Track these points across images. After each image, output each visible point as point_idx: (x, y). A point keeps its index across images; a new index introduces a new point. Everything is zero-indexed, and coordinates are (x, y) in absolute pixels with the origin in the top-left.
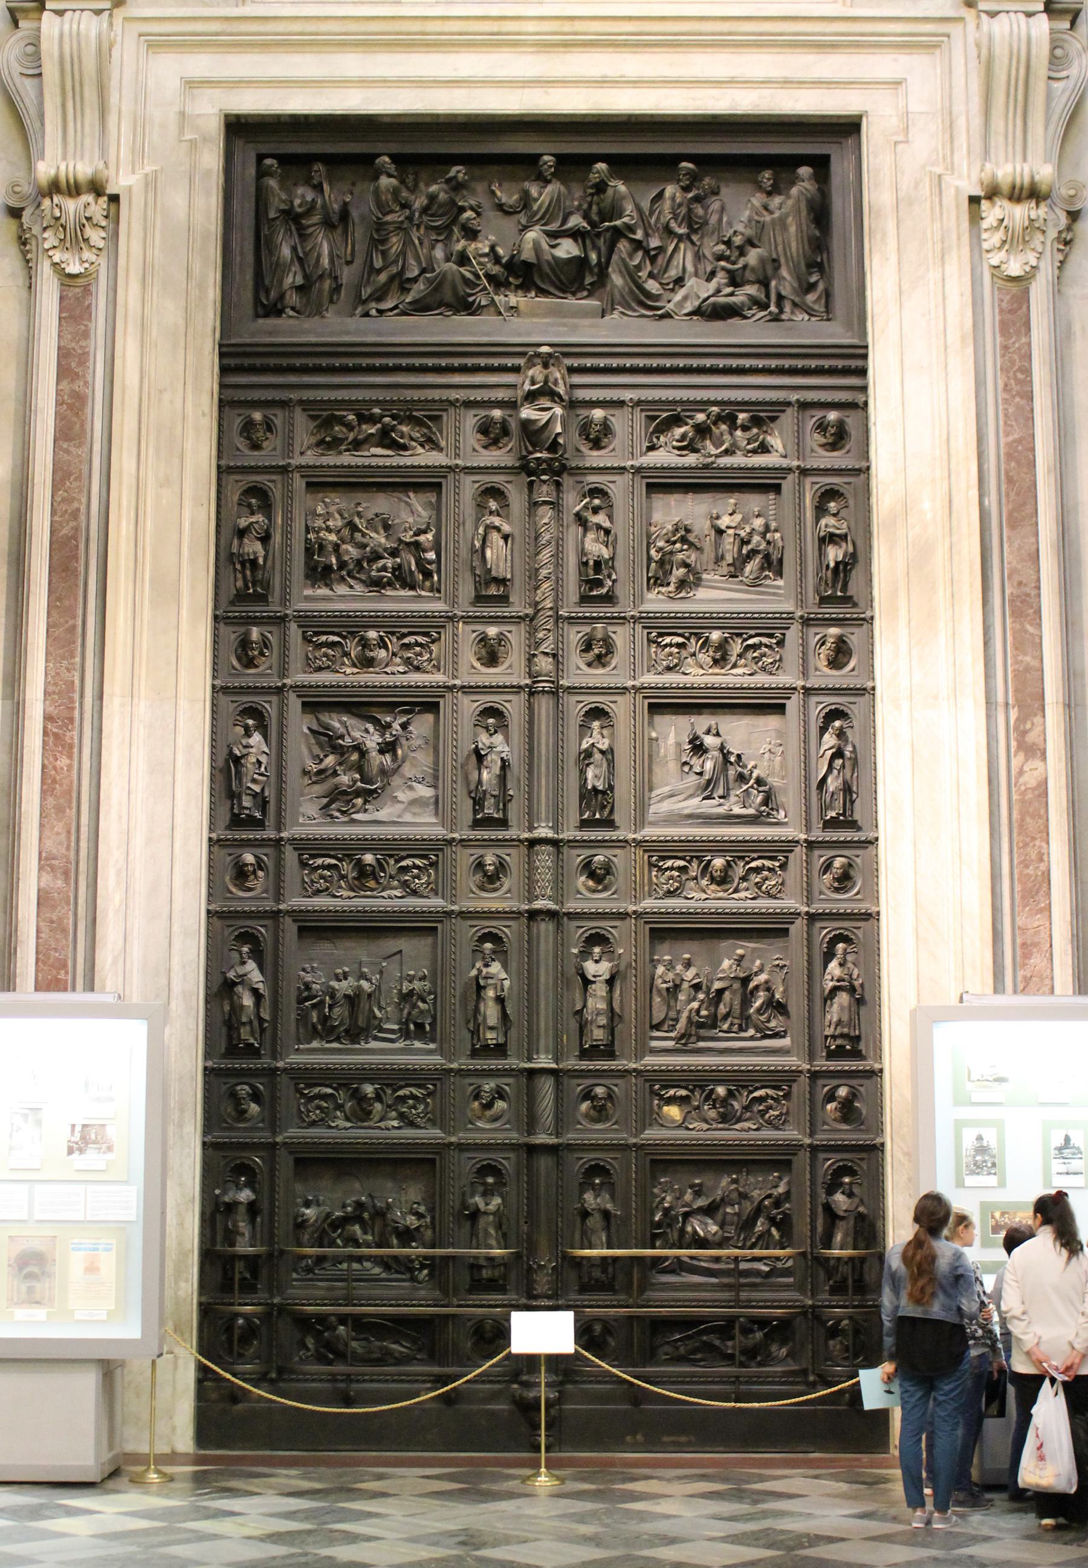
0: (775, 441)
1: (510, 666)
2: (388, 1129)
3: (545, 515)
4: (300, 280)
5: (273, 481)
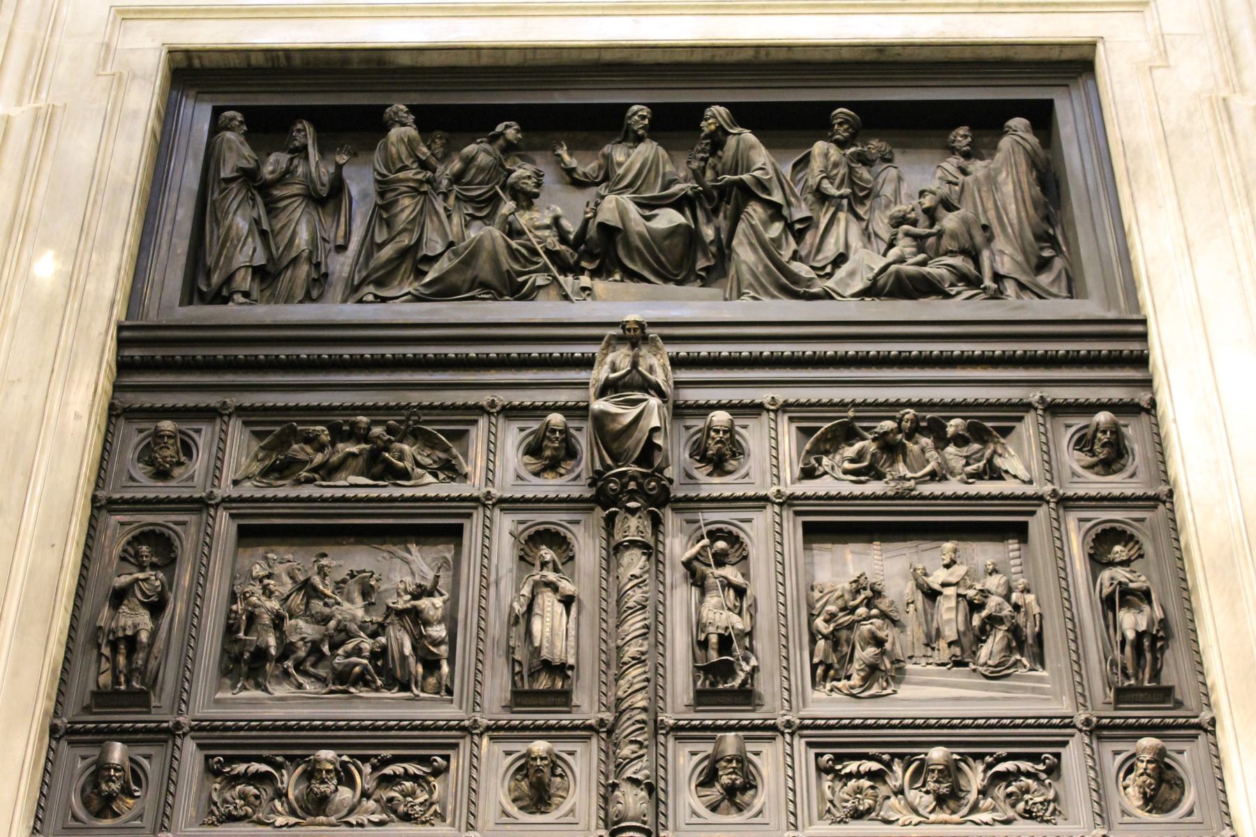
0: (1010, 462)
1: (572, 811)
4: (260, 259)
5: (184, 523)
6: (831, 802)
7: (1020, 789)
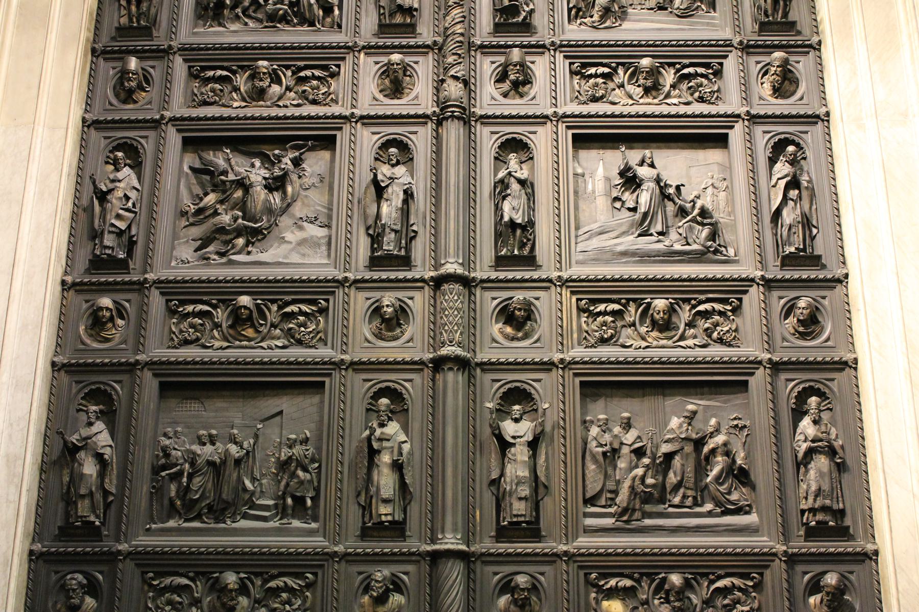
1: (417, 97)
6: (579, 92)
7: (697, 84)
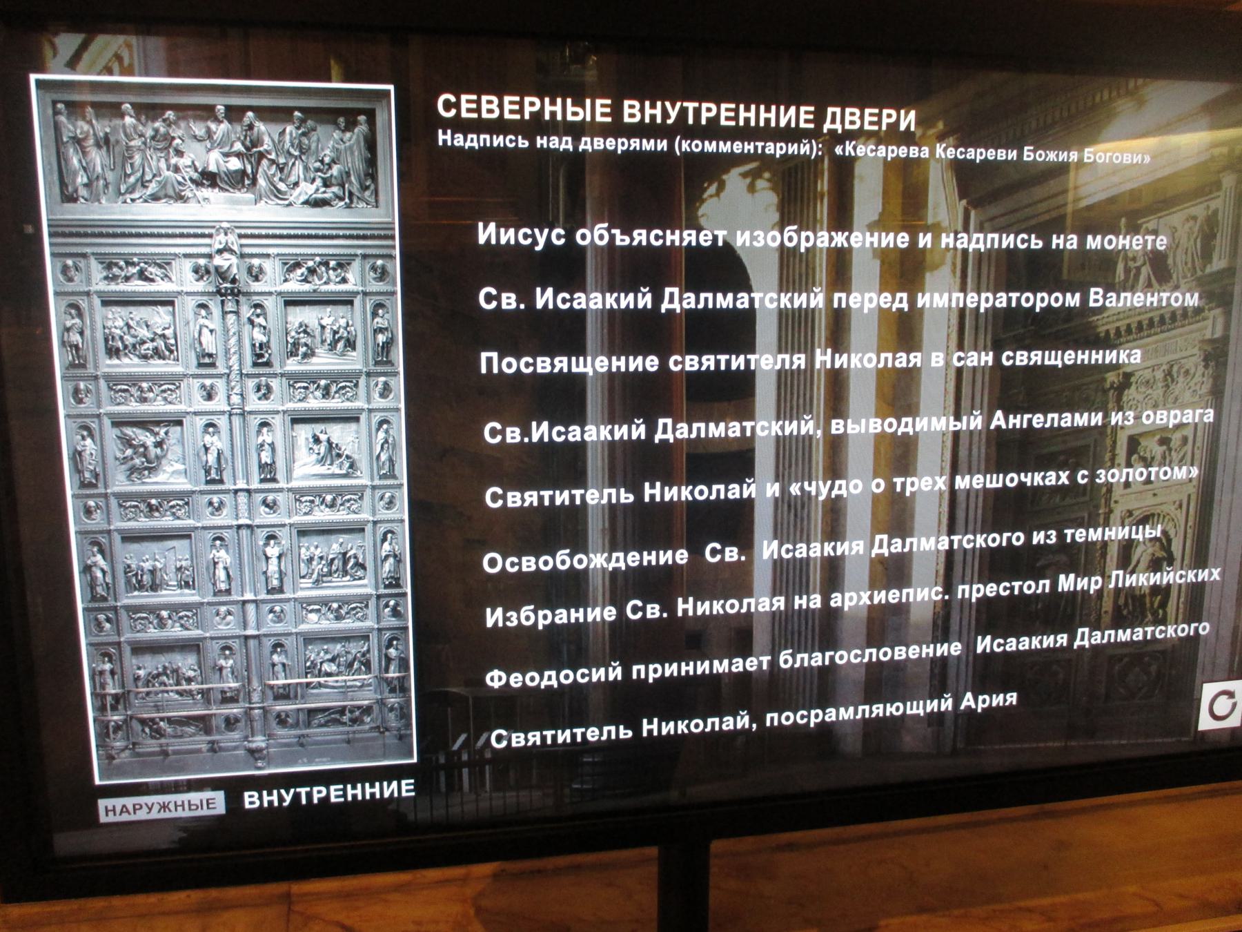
0: (350, 276)
2: (175, 631)
3: (231, 318)
